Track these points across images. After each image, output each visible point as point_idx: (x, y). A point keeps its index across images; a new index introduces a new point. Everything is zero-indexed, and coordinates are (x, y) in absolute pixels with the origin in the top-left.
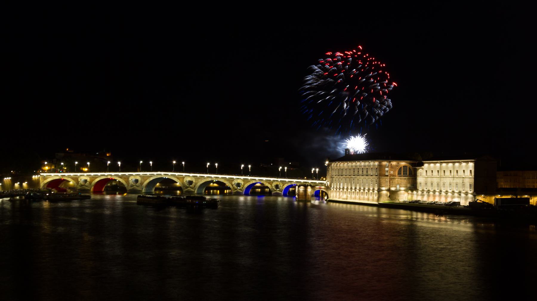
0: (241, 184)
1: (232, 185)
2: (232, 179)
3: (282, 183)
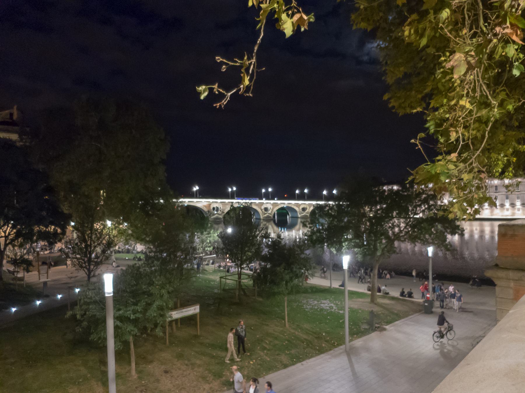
0: (271, 208)
1: (262, 210)
2: (261, 204)
3: (309, 206)
